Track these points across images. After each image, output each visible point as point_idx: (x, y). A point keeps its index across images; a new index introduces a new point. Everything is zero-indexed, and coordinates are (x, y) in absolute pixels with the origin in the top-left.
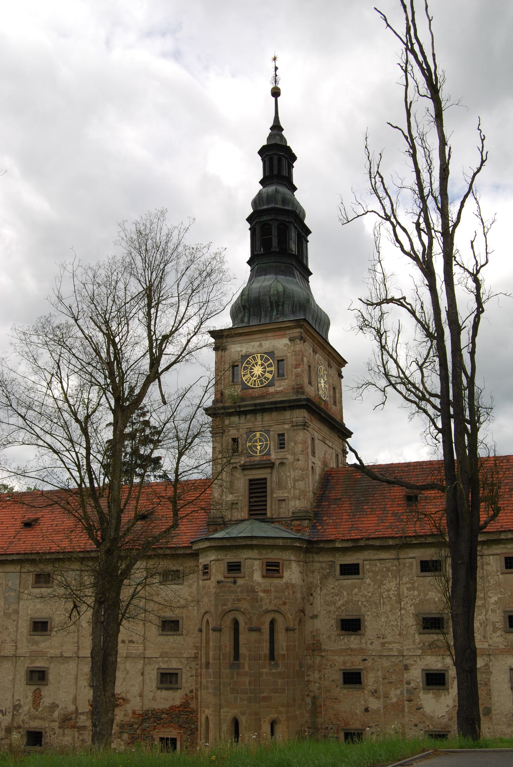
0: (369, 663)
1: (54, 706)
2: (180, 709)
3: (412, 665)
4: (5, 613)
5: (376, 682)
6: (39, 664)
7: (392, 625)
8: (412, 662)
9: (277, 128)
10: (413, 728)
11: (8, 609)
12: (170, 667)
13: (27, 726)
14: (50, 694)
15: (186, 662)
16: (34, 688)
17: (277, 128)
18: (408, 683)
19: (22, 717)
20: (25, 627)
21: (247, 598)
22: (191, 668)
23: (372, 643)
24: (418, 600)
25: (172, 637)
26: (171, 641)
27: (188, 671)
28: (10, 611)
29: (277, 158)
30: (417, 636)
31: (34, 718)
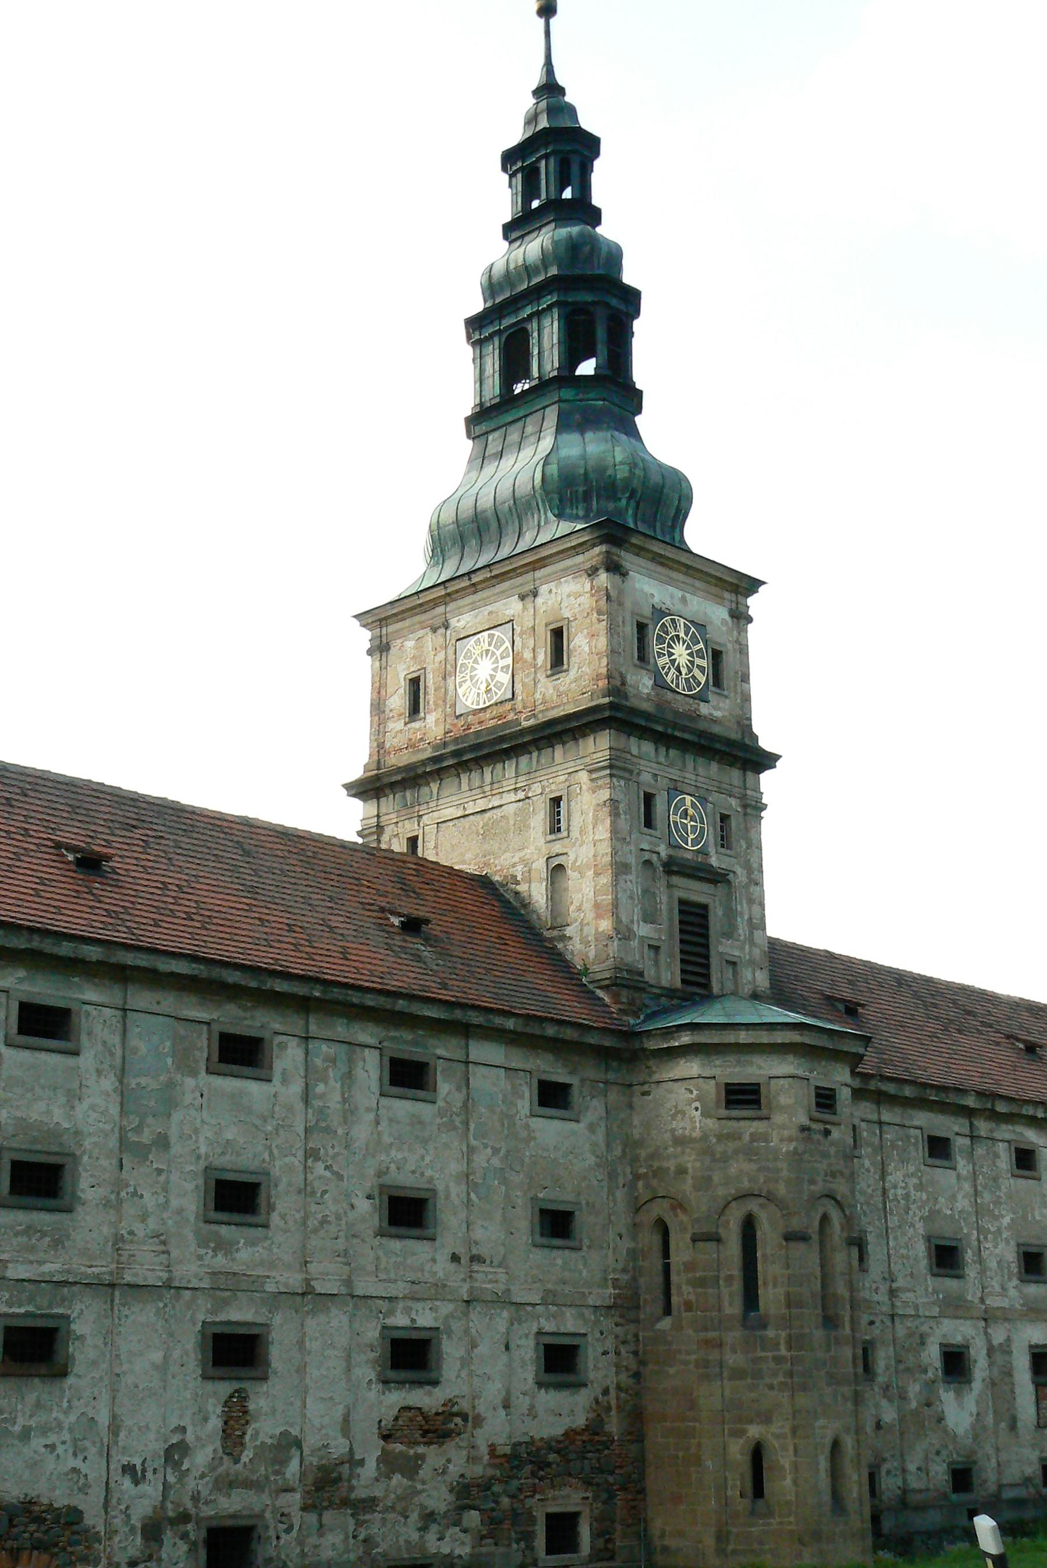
0: (876, 1331)
1: (288, 1443)
2: (584, 1438)
3: (929, 1335)
4: (123, 1142)
5: (887, 1368)
6: (240, 1313)
7: (903, 1256)
8: (929, 1331)
9: (550, 89)
10: (936, 1458)
11: (138, 1130)
12: (563, 1330)
13: (208, 1511)
14: (272, 1407)
15: (593, 1317)
16: (225, 1388)
17: (550, 89)
18: (926, 1371)
19: (191, 1484)
20: (188, 1197)
21: (845, 1171)
22: (602, 1333)
23: (877, 1288)
24: (927, 1209)
25: (560, 1252)
26: (558, 1262)
27: (598, 1340)
28: (146, 1137)
29: (554, 158)
30: (929, 1277)
31: (227, 1484)
